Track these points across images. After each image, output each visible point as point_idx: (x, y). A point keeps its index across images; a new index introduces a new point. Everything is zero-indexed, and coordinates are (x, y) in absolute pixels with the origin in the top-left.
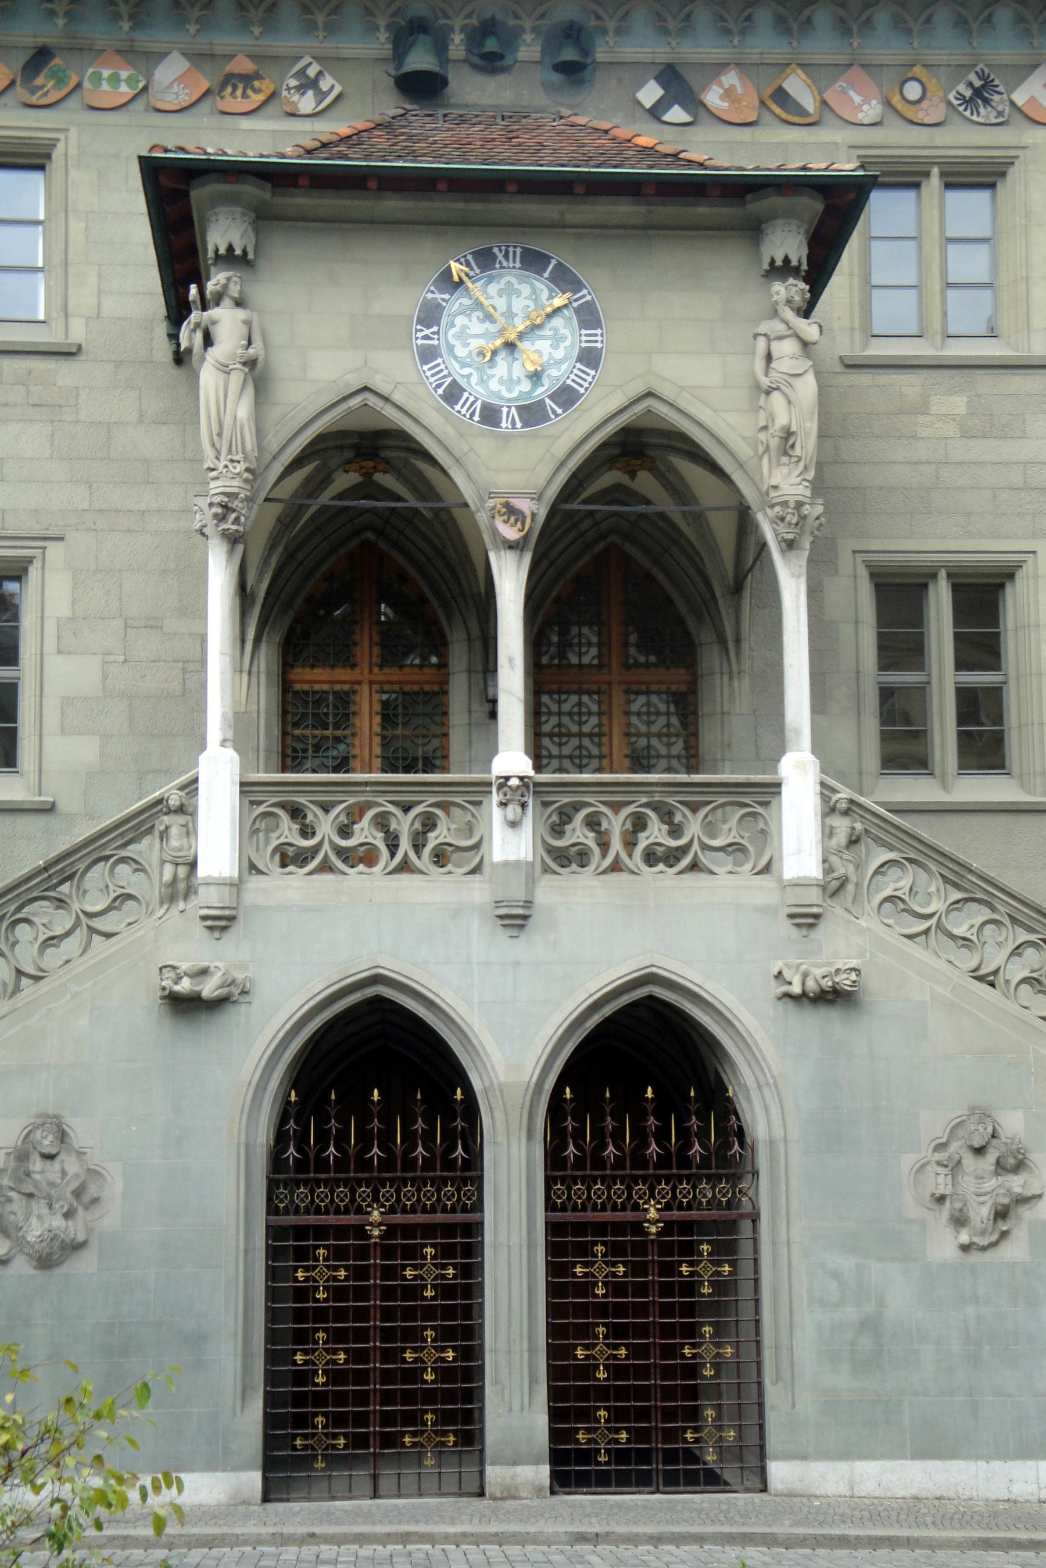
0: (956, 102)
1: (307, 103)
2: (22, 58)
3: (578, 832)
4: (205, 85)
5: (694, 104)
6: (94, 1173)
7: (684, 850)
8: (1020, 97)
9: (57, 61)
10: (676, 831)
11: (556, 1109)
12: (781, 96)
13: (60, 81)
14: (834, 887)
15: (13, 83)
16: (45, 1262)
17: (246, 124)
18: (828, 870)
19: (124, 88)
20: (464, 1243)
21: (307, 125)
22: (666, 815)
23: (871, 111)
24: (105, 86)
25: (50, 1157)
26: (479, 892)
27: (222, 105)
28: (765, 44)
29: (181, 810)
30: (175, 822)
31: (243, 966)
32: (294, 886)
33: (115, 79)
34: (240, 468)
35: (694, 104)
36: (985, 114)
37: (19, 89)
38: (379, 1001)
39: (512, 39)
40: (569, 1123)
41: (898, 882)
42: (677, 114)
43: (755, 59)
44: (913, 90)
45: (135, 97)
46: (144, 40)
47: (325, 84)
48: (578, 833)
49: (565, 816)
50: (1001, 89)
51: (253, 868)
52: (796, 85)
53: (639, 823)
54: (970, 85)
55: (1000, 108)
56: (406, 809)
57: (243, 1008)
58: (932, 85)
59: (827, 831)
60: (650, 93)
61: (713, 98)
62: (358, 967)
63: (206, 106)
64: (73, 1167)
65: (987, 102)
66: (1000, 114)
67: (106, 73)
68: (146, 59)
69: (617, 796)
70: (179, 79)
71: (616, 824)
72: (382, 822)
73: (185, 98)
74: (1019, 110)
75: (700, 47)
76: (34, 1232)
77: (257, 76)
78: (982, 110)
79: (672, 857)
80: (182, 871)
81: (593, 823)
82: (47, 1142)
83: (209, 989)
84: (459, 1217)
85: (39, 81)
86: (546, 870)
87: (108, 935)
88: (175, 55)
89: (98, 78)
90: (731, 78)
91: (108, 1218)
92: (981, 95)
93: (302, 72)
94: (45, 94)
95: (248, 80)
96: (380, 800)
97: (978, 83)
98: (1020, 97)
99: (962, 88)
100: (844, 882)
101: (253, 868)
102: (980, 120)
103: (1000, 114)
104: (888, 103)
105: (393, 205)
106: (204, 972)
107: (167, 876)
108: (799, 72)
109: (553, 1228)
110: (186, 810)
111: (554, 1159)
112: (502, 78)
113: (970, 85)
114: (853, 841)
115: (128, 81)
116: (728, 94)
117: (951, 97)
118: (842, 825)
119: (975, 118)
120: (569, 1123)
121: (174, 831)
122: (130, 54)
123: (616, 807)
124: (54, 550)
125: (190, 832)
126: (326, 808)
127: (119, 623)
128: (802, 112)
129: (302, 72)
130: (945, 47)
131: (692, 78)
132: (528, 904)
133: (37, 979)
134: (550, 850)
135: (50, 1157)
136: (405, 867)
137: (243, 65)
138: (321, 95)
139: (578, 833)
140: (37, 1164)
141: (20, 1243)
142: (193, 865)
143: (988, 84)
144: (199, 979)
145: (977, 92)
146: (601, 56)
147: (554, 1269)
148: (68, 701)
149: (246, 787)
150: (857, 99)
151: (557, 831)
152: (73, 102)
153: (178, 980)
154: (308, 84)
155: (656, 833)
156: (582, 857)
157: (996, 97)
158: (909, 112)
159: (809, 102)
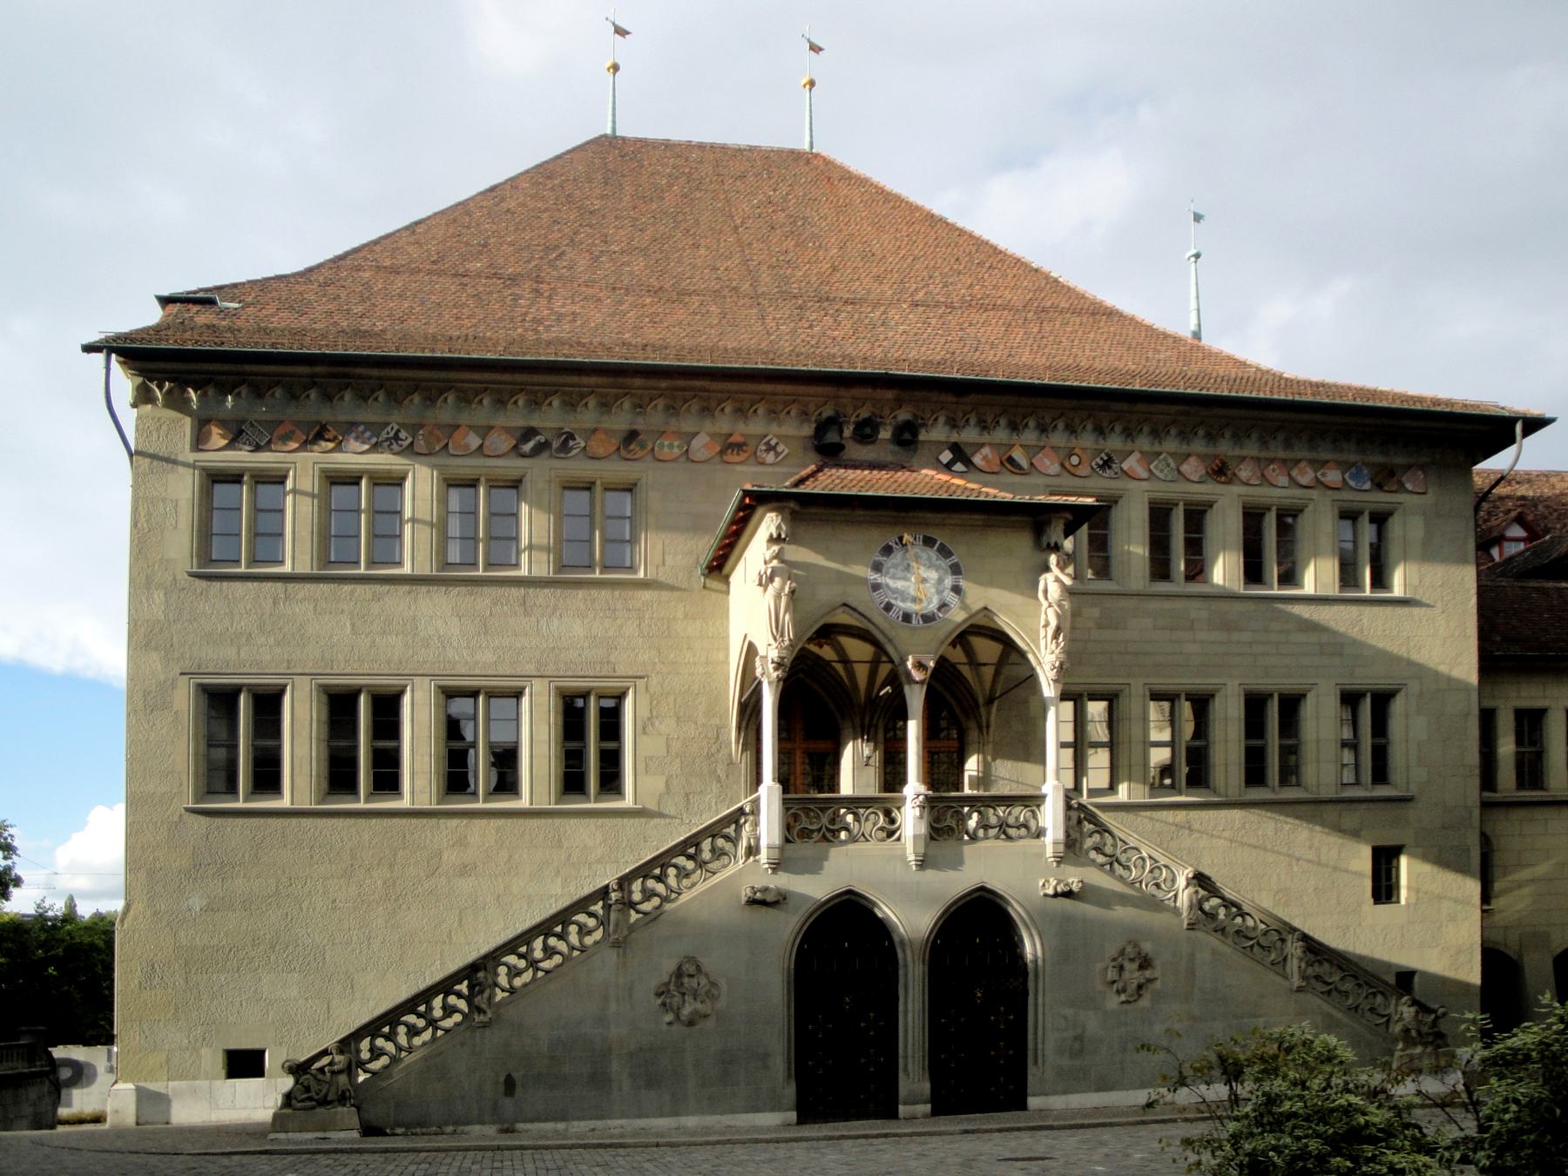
1: (770, 457)
5: (968, 462)
6: (713, 984)
8: (1125, 466)
12: (1011, 460)
13: (643, 447)
16: (691, 1023)
17: (739, 468)
19: (676, 451)
21: (770, 469)
23: (1055, 468)
25: (691, 976)
28: (1001, 434)
33: (671, 446)
35: (968, 462)
42: (959, 467)
44: (1075, 460)
46: (687, 425)
47: (779, 449)
52: (1018, 455)
58: (1084, 458)
60: (946, 456)
61: (977, 459)
64: (703, 981)
74: (1125, 472)
75: (969, 435)
76: (686, 1011)
77: (744, 444)
82: (692, 970)
89: (662, 446)
90: (986, 451)
91: (721, 1004)
92: (1107, 464)
93: (768, 443)
95: (739, 447)
98: (1125, 466)
104: (1062, 465)
112: (870, 447)
114: (1080, 822)
116: (985, 458)
118: (1074, 815)
122: (678, 434)
124: (641, 683)
128: (1019, 467)
129: (768, 443)
130: (1087, 440)
131: (968, 450)
134: (932, 827)
135: (691, 976)
137: (736, 438)
138: (777, 454)
140: (686, 980)
141: (678, 1017)
150: (1048, 463)
154: (771, 448)
159: (1024, 463)
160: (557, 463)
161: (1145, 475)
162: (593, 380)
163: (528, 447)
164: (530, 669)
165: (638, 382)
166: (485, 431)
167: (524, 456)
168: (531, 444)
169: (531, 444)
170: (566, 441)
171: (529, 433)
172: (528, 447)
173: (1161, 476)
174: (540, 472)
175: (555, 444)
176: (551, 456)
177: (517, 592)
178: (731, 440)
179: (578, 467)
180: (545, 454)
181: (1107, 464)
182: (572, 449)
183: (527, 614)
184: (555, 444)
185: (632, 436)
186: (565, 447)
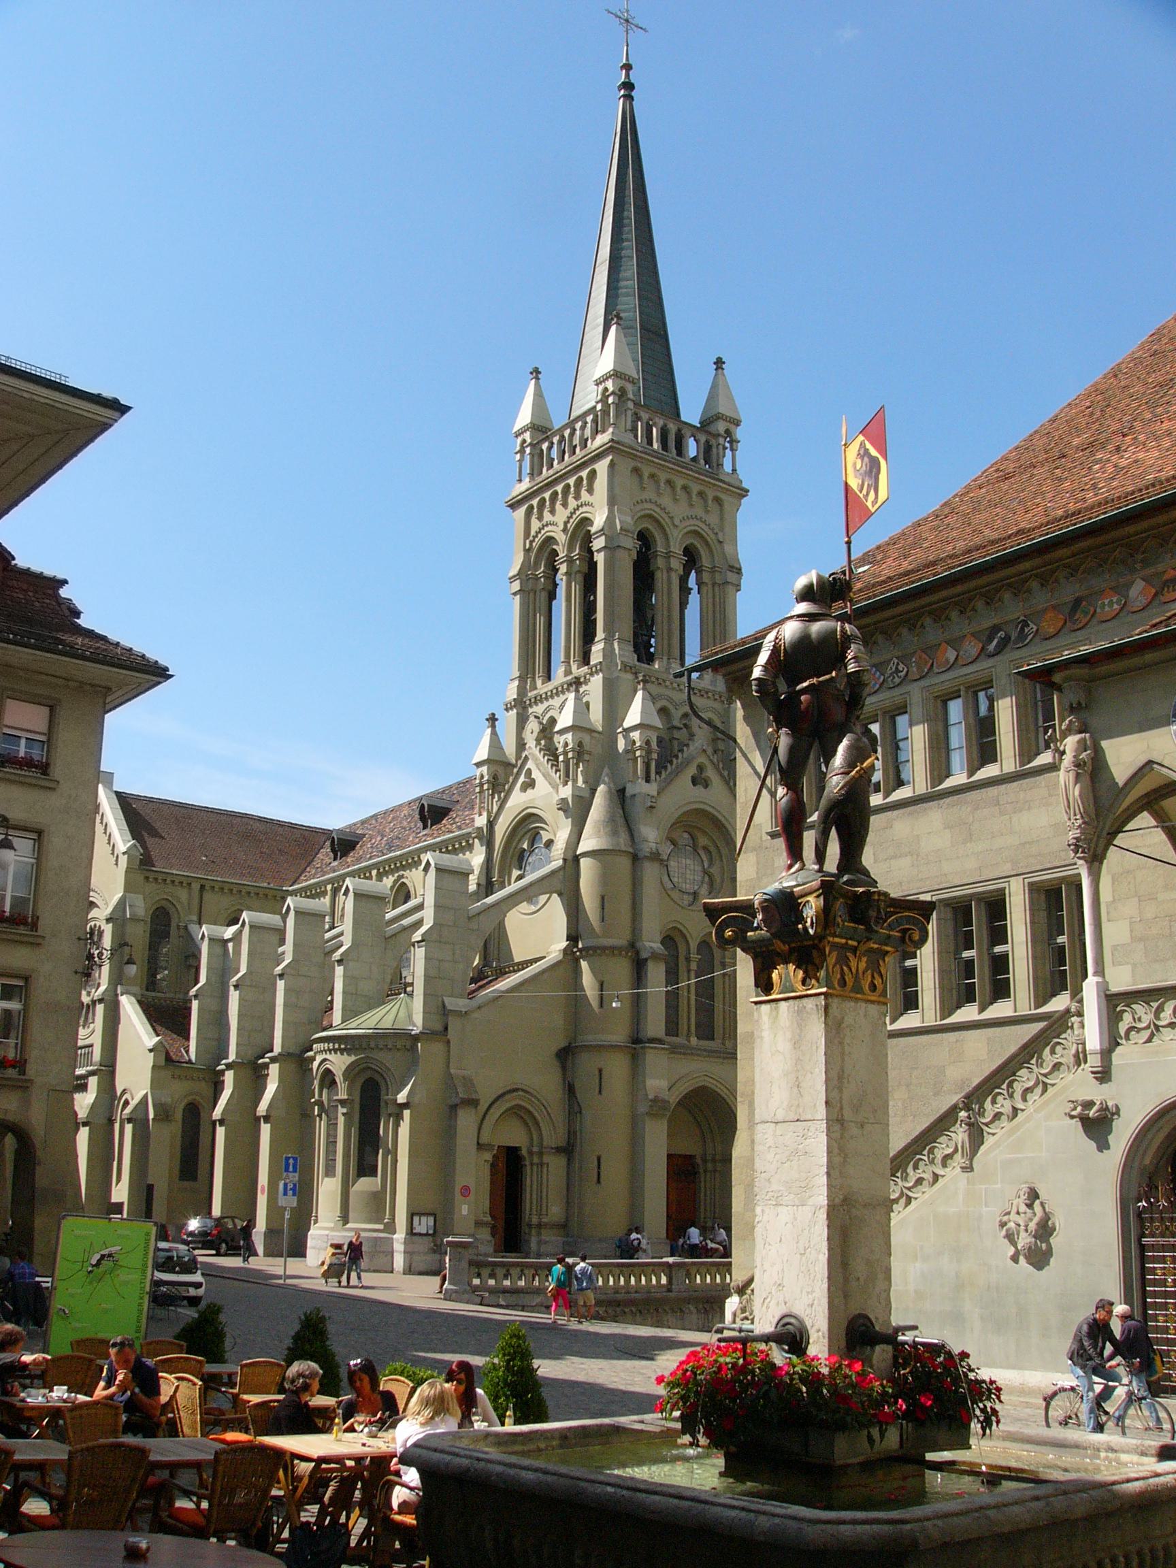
4: (1153, 591)
19: (1115, 606)
24: (1107, 609)
27: (1163, 599)
34: (1080, 822)
37: (1068, 624)
45: (1121, 609)
63: (1156, 603)
67: (1106, 602)
68: (1121, 590)
70: (1141, 593)
73: (1145, 602)
87: (1053, 1085)
88: (1138, 580)
105: (1149, 657)
107: (1073, 1051)
110: (1080, 1014)
115: (1117, 603)
121: (1075, 1026)
122: (1115, 589)
127: (1136, 899)
142: (1084, 1044)
148: (1114, 948)
152: (1094, 621)
162: (1027, 565)
164: (1007, 869)
165: (1063, 552)
166: (955, 643)
168: (995, 642)
169: (995, 642)
170: (1022, 629)
171: (995, 629)
174: (1003, 667)
175: (1014, 635)
176: (1012, 649)
177: (993, 791)
178: (1165, 577)
180: (1010, 645)
182: (1027, 636)
183: (1002, 813)
184: (1014, 635)
185: (1077, 602)
186: (1022, 636)
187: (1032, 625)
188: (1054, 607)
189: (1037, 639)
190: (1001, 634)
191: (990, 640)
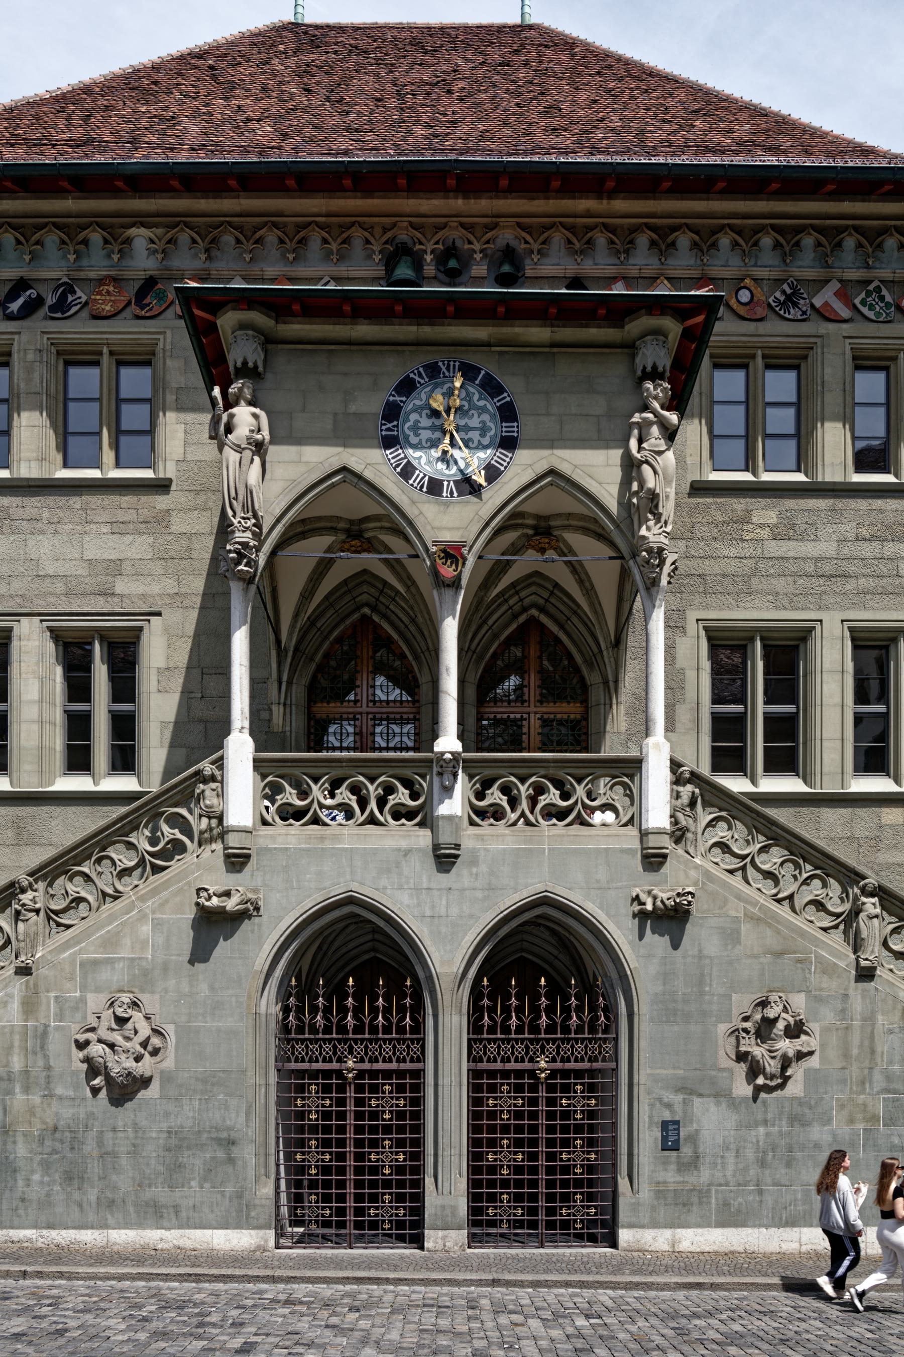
0: (774, 304)
2: (137, 287)
3: (495, 795)
7: (569, 810)
8: (818, 302)
9: (160, 286)
10: (565, 796)
11: (476, 993)
14: (679, 835)
15: (129, 303)
18: (676, 823)
20: (412, 1084)
22: (559, 784)
26: (423, 838)
29: (213, 779)
30: (208, 789)
31: (256, 891)
32: (293, 834)
36: (794, 313)
38: (353, 915)
39: (466, 262)
40: (486, 1002)
41: (721, 832)
43: (635, 272)
44: (745, 296)
48: (495, 796)
49: (487, 784)
50: (805, 296)
51: (265, 823)
53: (540, 790)
54: (784, 292)
55: (804, 309)
56: (372, 780)
57: (256, 920)
58: (758, 292)
59: (675, 794)
62: (336, 890)
65: (795, 305)
66: (804, 313)
69: (524, 771)
71: (524, 790)
72: (355, 789)
78: (792, 310)
79: (561, 815)
80: (214, 822)
81: (506, 790)
83: (231, 904)
84: (408, 1066)
85: (146, 301)
86: (472, 823)
92: (791, 300)
94: (151, 309)
96: (353, 773)
97: (789, 291)
99: (778, 294)
100: (684, 831)
101: (265, 823)
102: (790, 317)
103: (804, 313)
106: (227, 894)
108: (666, 282)
109: (474, 1074)
110: (217, 779)
111: (475, 1027)
113: (784, 292)
114: (692, 804)
117: (771, 300)
119: (787, 315)
120: (486, 1002)
123: (523, 780)
125: (221, 795)
126: (316, 780)
132: (457, 846)
133: (116, 898)
136: (372, 820)
139: (495, 796)
142: (220, 818)
143: (796, 292)
144: (224, 898)
145: (789, 298)
146: (529, 273)
147: (475, 1102)
149: (258, 764)
151: (480, 796)
153: (209, 898)
155: (553, 796)
156: (497, 814)
157: (802, 302)
158: (742, 311)
160: (53, 326)
161: (845, 313)
163: (15, 306)
167: (10, 317)
168: (21, 301)
169: (21, 301)
172: (15, 306)
173: (871, 315)
175: (50, 300)
179: (78, 329)
181: (791, 300)
187: (79, 293)
188: (115, 280)
189: (85, 314)
190: (32, 293)
191: (12, 295)
